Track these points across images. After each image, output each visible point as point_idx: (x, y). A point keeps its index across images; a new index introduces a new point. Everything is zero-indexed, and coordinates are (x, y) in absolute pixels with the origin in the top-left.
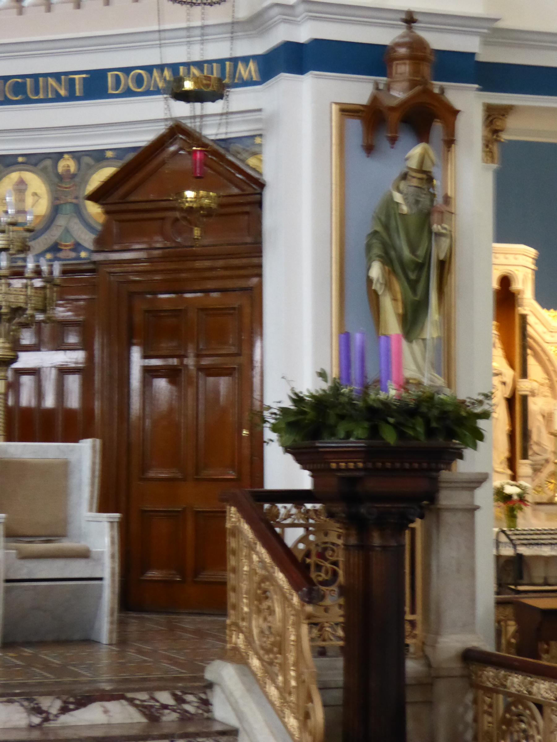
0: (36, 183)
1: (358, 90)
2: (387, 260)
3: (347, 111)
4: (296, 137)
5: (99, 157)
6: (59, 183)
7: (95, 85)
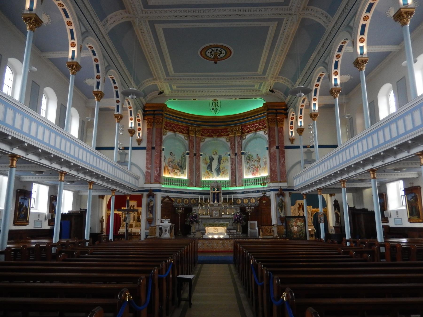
0: (254, 199)
1: (277, 192)
2: (279, 206)
3: (276, 194)
4: (272, 195)
5: (258, 197)
6: (255, 199)
7: (258, 192)
